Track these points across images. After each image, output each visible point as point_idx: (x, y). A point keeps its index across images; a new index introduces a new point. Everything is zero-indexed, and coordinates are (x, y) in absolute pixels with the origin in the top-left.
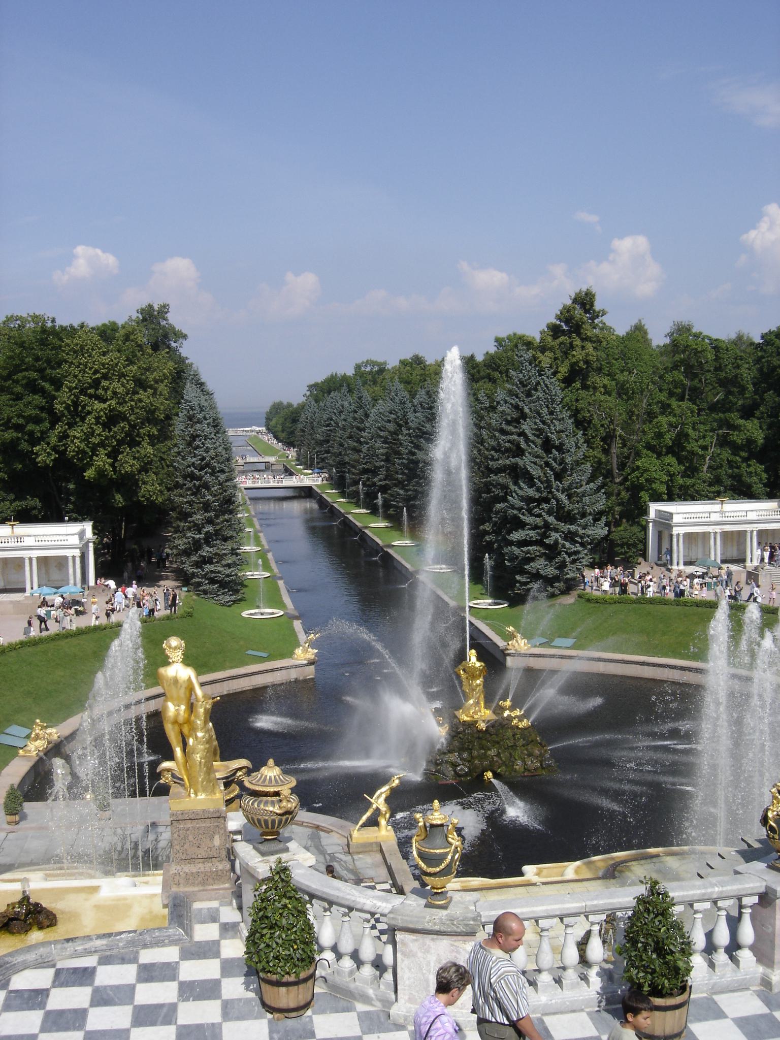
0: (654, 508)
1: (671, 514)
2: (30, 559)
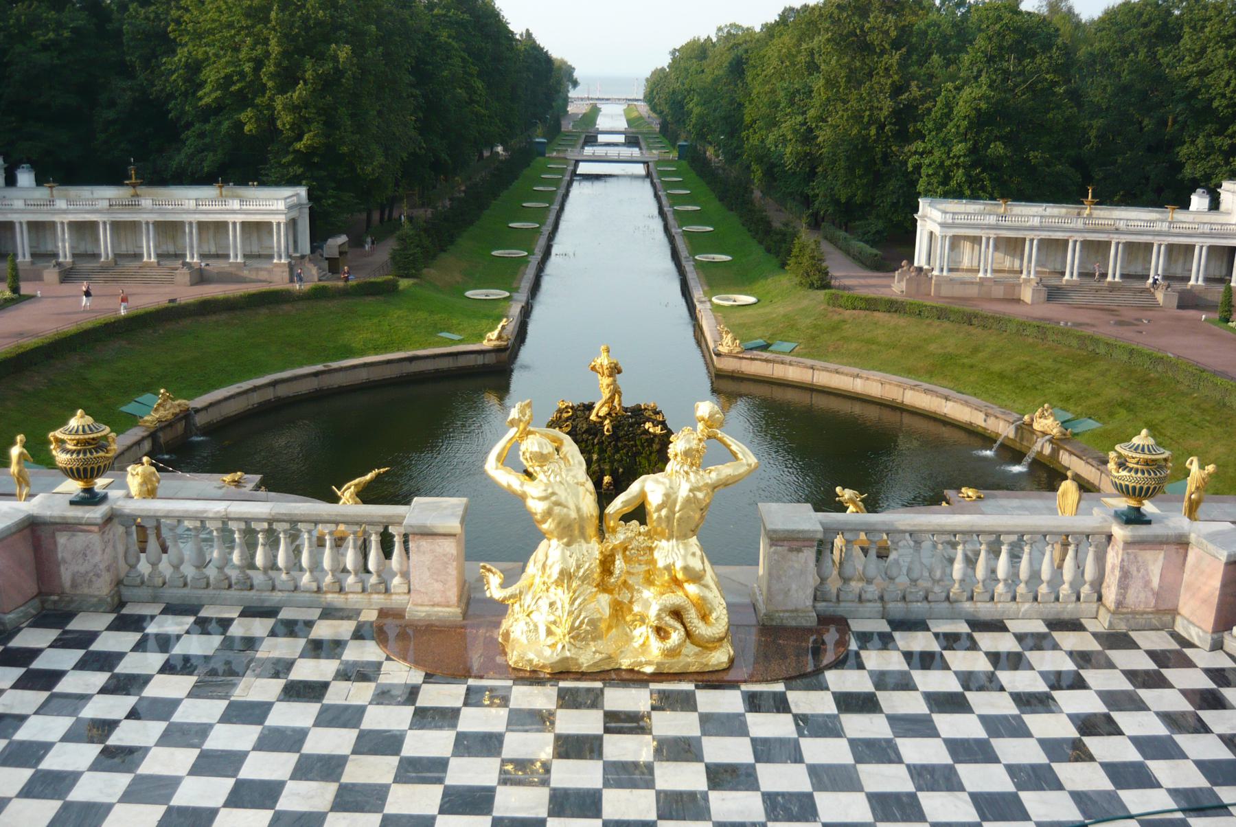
2: (234, 223)
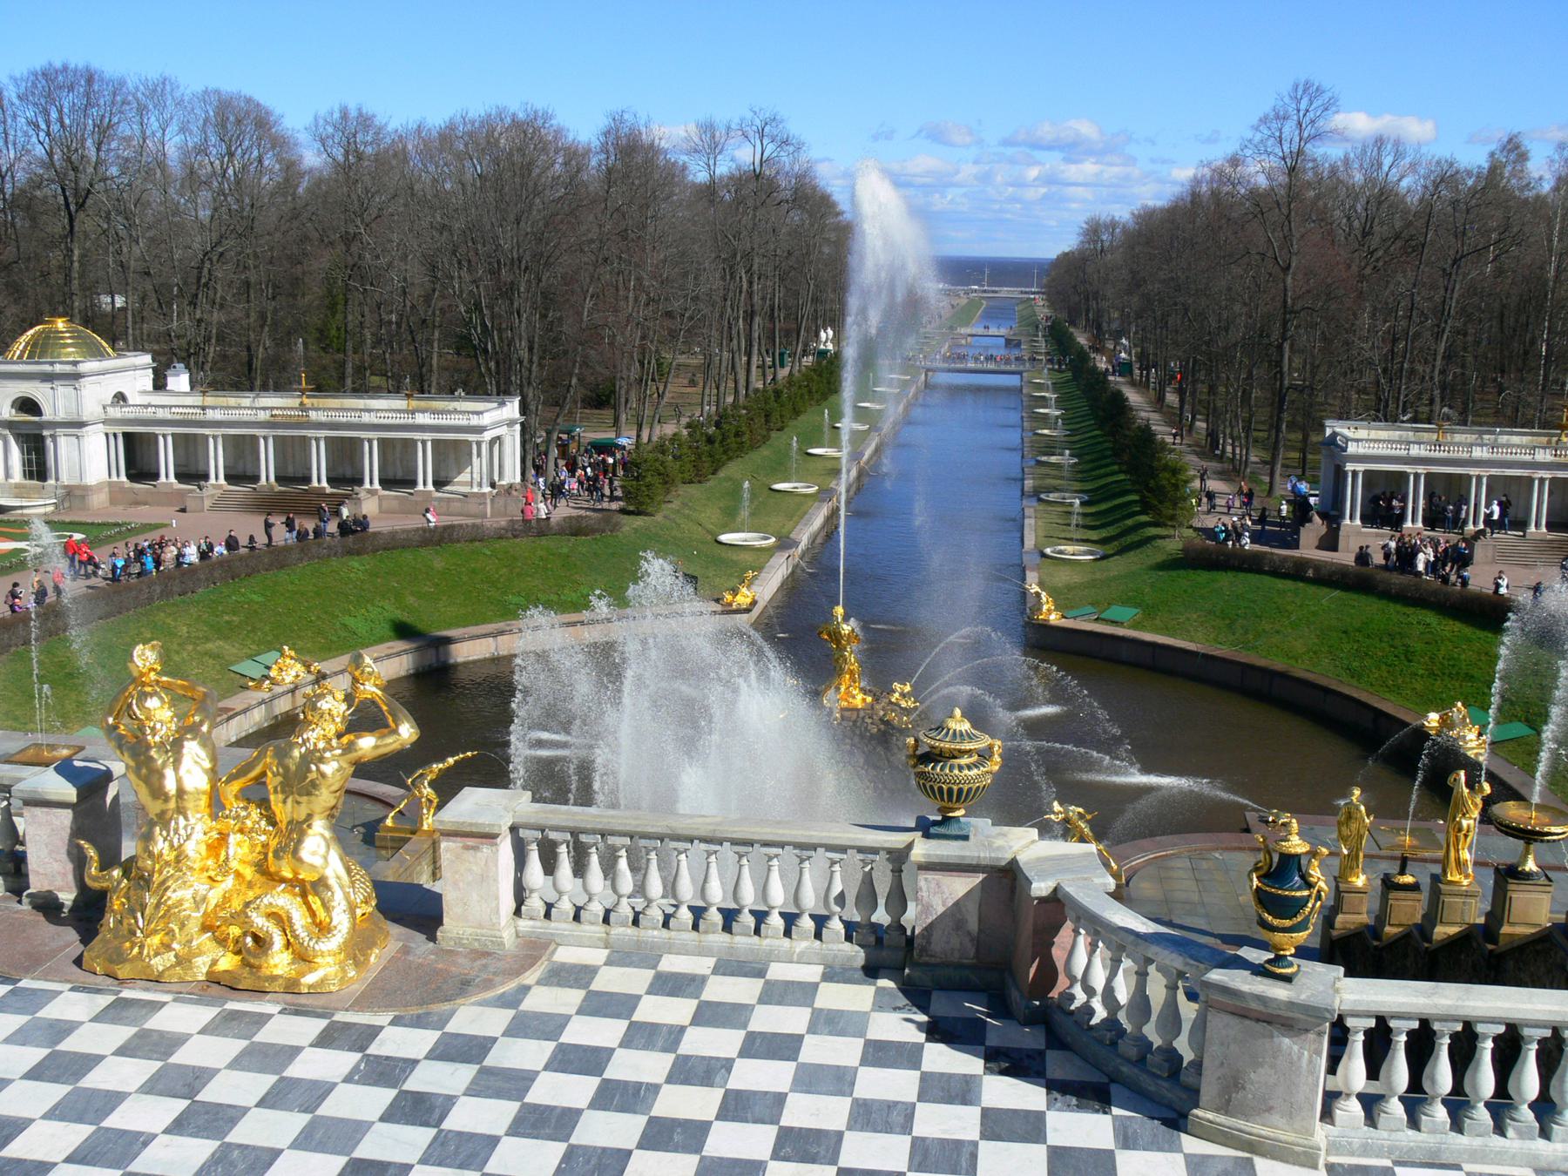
0: (1333, 427)
1: (1347, 440)
2: (424, 442)
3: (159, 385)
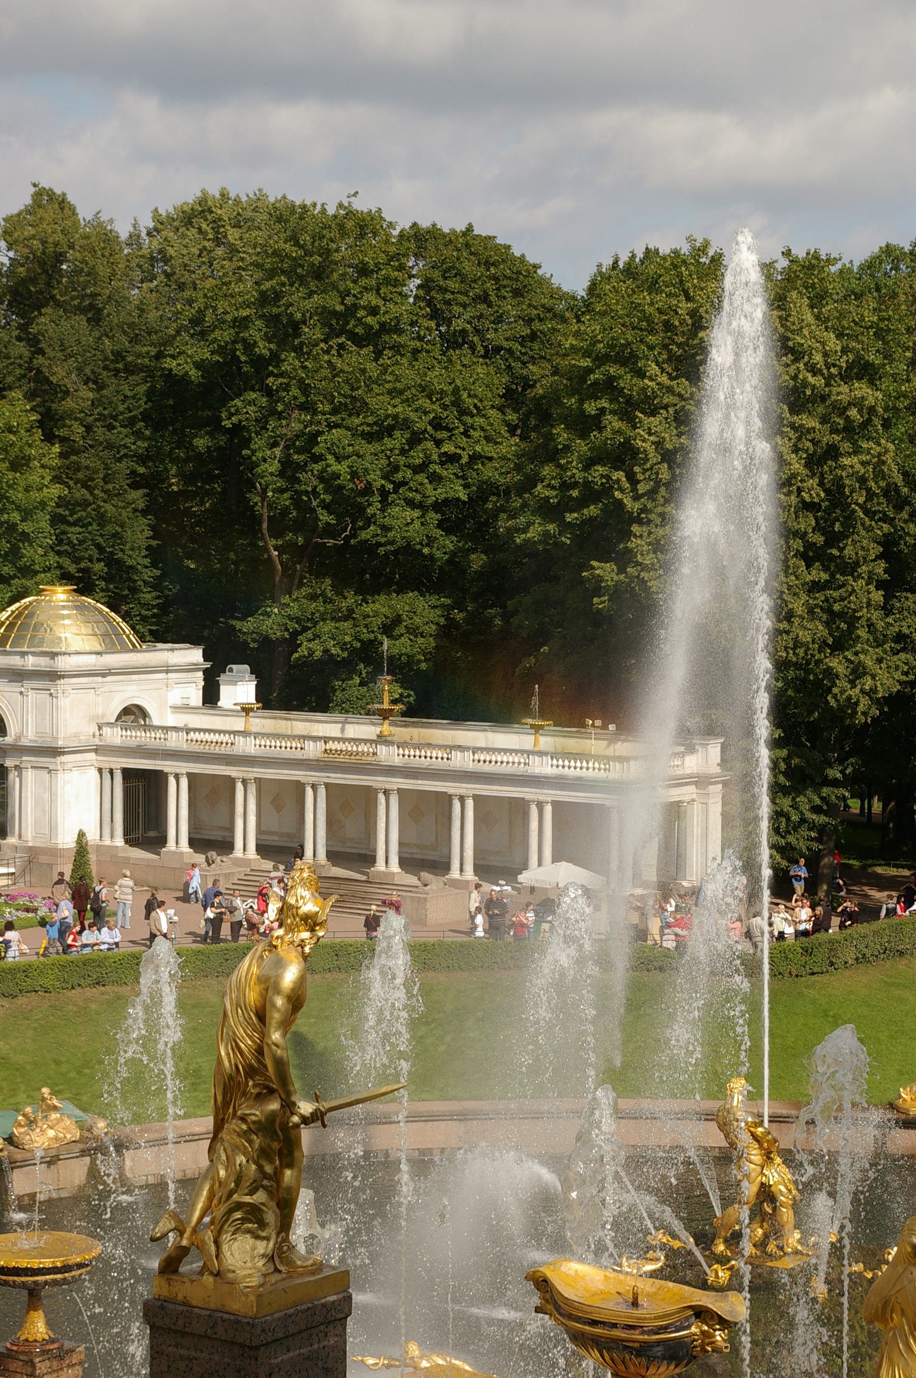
3: (211, 696)
